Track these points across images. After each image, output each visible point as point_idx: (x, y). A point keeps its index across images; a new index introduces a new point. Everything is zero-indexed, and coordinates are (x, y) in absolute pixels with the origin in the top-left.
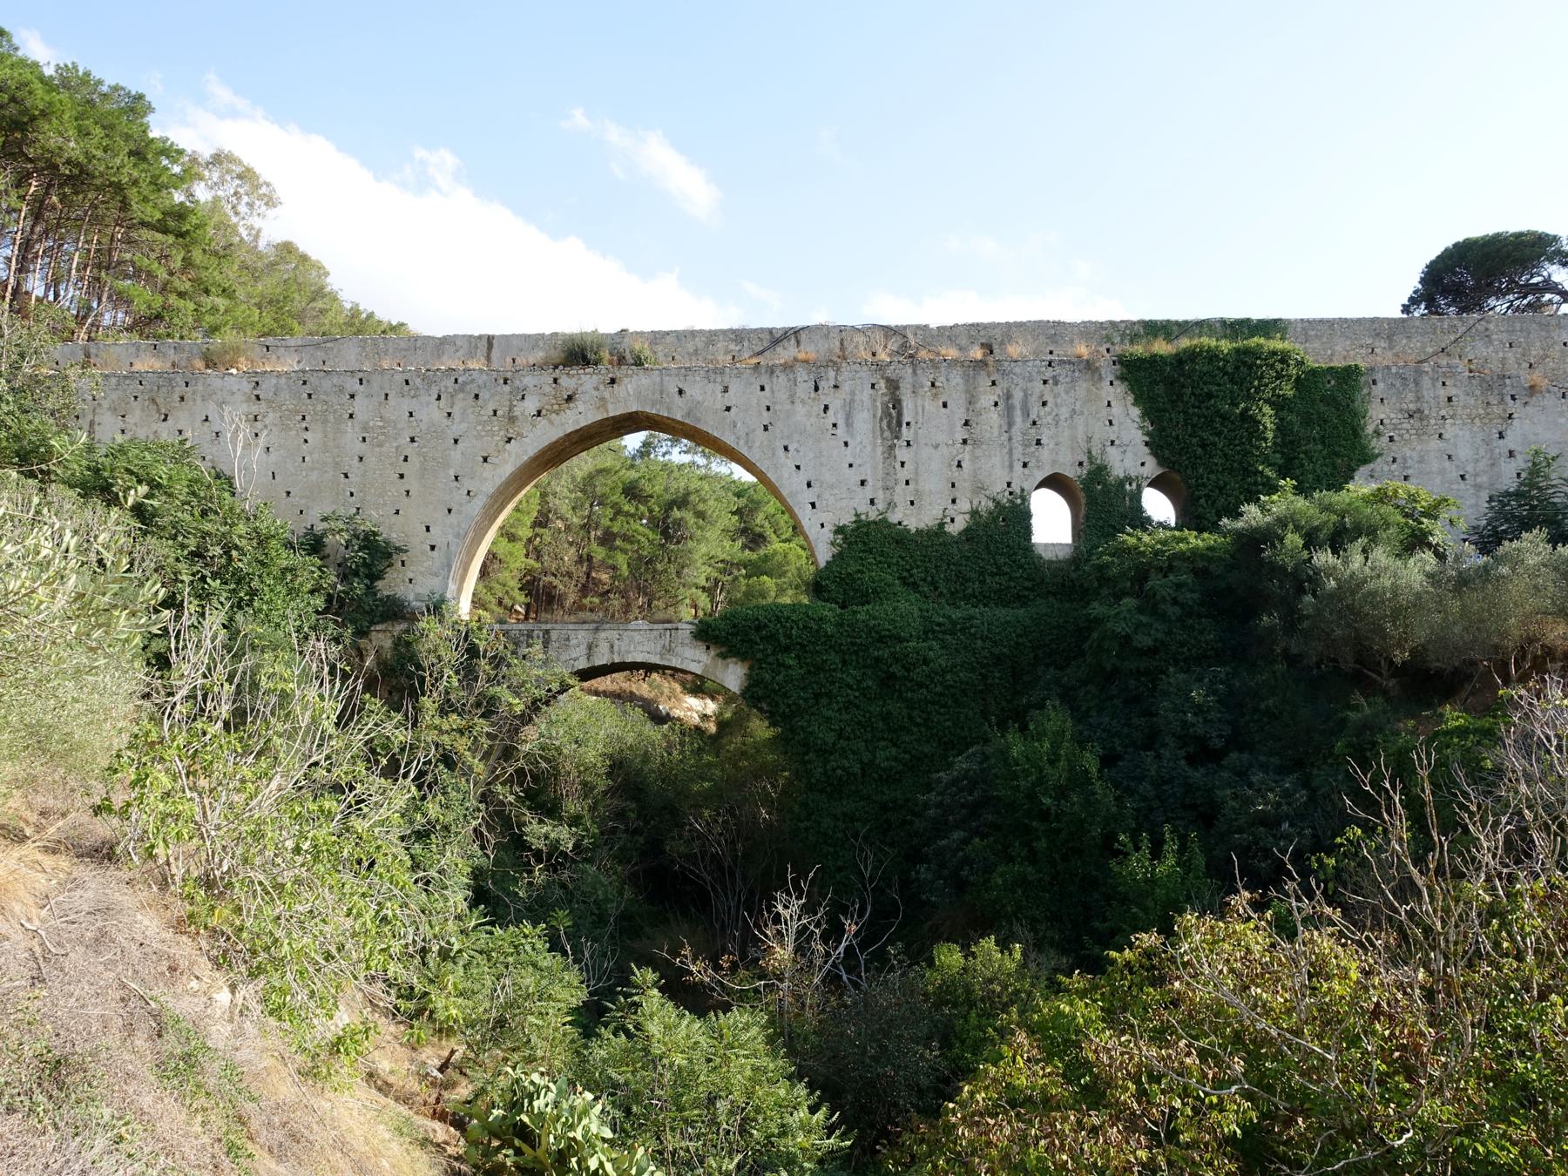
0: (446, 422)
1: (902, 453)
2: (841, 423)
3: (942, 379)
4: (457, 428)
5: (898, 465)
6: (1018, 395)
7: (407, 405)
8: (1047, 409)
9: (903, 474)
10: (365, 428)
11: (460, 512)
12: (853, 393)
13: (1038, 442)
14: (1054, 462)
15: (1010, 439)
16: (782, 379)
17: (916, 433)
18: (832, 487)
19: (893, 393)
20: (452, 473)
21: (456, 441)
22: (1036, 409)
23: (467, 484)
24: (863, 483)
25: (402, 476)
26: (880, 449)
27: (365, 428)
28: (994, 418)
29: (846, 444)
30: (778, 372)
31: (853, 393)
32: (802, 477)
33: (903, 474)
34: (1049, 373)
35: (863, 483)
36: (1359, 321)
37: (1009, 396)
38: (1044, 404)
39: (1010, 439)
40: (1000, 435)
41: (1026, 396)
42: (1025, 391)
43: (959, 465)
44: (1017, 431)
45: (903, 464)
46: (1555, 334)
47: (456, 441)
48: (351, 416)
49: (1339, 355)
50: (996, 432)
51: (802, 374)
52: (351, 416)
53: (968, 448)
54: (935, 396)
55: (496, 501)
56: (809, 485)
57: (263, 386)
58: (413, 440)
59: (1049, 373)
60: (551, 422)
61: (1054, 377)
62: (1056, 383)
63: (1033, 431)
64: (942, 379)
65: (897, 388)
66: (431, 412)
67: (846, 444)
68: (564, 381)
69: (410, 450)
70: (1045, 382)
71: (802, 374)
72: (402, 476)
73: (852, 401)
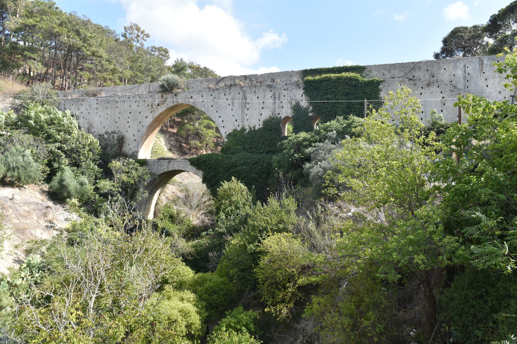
0: (137, 108)
1: (246, 112)
2: (231, 104)
3: (257, 90)
4: (140, 109)
5: (245, 115)
6: (277, 94)
7: (129, 104)
8: (285, 97)
9: (246, 117)
10: (120, 110)
11: (141, 131)
12: (234, 96)
13: (283, 107)
14: (287, 113)
15: (275, 107)
16: (216, 92)
17: (250, 106)
18: (228, 122)
19: (244, 95)
20: (139, 121)
21: (140, 113)
22: (282, 98)
23: (142, 124)
24: (236, 120)
25: (128, 122)
26: (241, 111)
27: (120, 110)
28: (271, 101)
29: (232, 110)
30: (215, 91)
31: (234, 96)
32: (221, 119)
33: (246, 117)
34: (286, 87)
35: (236, 120)
36: (380, 66)
37: (274, 94)
38: (284, 96)
39: (275, 107)
40: (272, 106)
41: (279, 94)
42: (279, 93)
43: (261, 115)
44: (277, 105)
45: (247, 115)
46: (441, 66)
47: (140, 113)
48: (117, 107)
49: (376, 76)
50: (271, 105)
51: (221, 91)
52: (117, 107)
53: (263, 109)
54: (255, 95)
55: (151, 128)
56: (223, 121)
57: (98, 100)
58: (130, 113)
59: (286, 87)
60: (161, 107)
61: (287, 88)
62: (288, 90)
63: (281, 104)
64: (257, 90)
65: (245, 93)
66: (135, 106)
67: (232, 110)
68: (164, 96)
69: (130, 115)
70: (285, 90)
71: (221, 91)
72: (128, 122)
73: (234, 98)
